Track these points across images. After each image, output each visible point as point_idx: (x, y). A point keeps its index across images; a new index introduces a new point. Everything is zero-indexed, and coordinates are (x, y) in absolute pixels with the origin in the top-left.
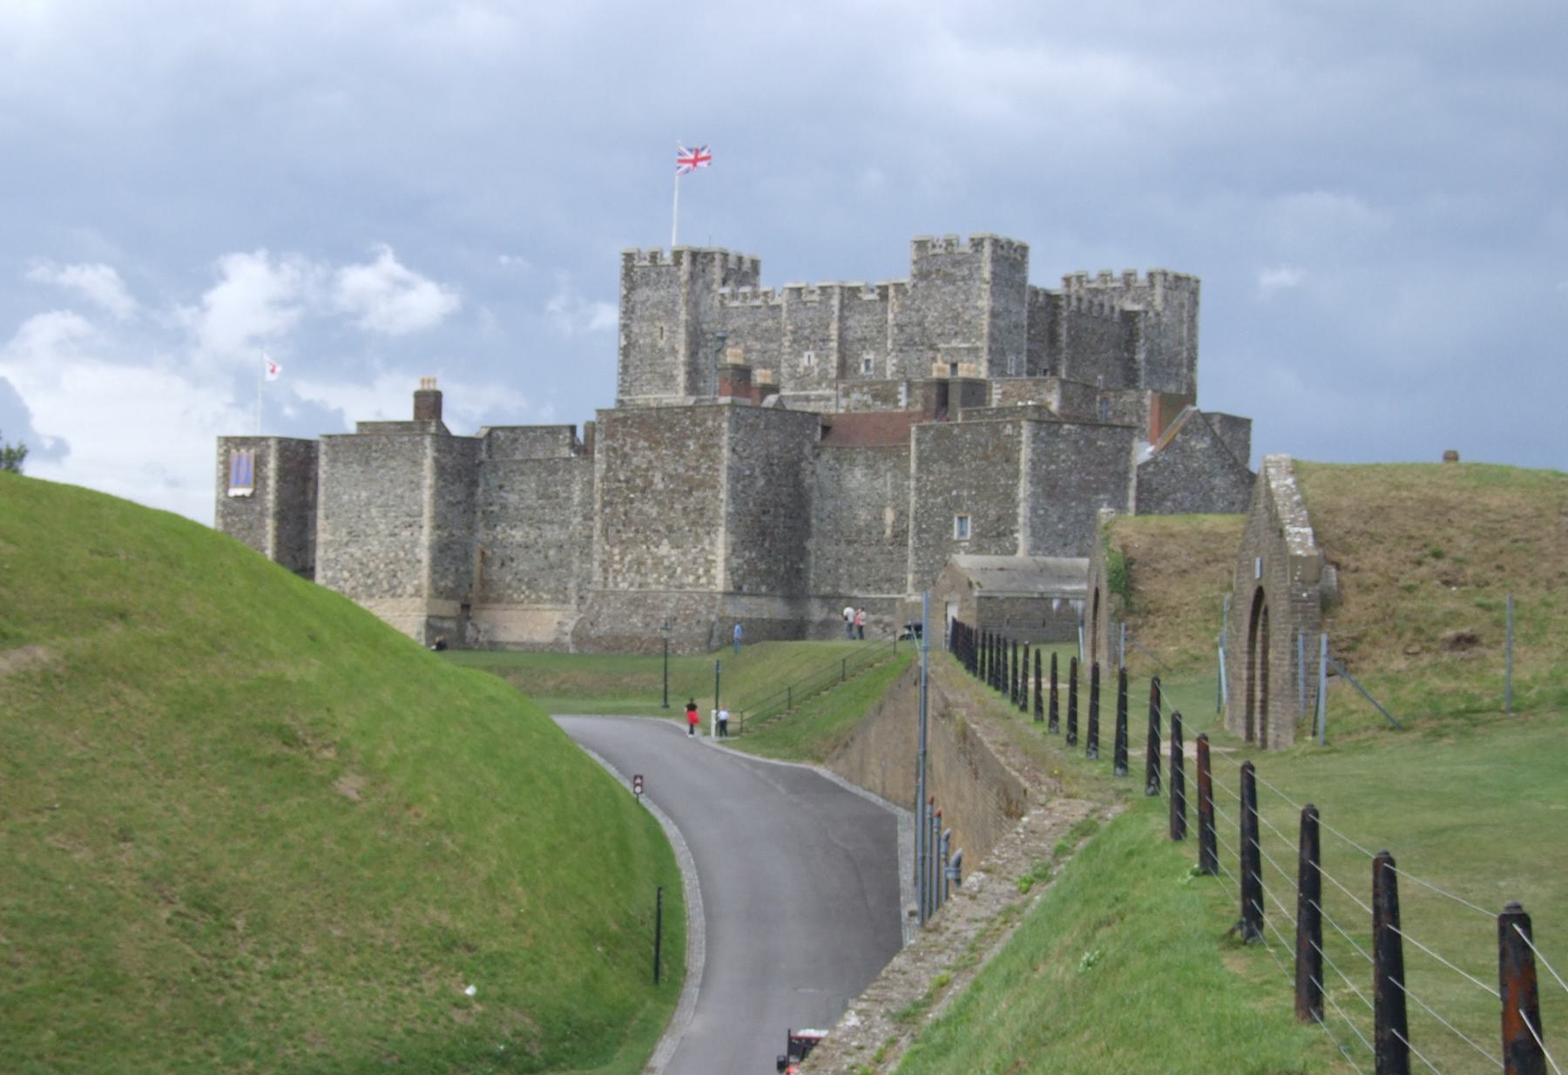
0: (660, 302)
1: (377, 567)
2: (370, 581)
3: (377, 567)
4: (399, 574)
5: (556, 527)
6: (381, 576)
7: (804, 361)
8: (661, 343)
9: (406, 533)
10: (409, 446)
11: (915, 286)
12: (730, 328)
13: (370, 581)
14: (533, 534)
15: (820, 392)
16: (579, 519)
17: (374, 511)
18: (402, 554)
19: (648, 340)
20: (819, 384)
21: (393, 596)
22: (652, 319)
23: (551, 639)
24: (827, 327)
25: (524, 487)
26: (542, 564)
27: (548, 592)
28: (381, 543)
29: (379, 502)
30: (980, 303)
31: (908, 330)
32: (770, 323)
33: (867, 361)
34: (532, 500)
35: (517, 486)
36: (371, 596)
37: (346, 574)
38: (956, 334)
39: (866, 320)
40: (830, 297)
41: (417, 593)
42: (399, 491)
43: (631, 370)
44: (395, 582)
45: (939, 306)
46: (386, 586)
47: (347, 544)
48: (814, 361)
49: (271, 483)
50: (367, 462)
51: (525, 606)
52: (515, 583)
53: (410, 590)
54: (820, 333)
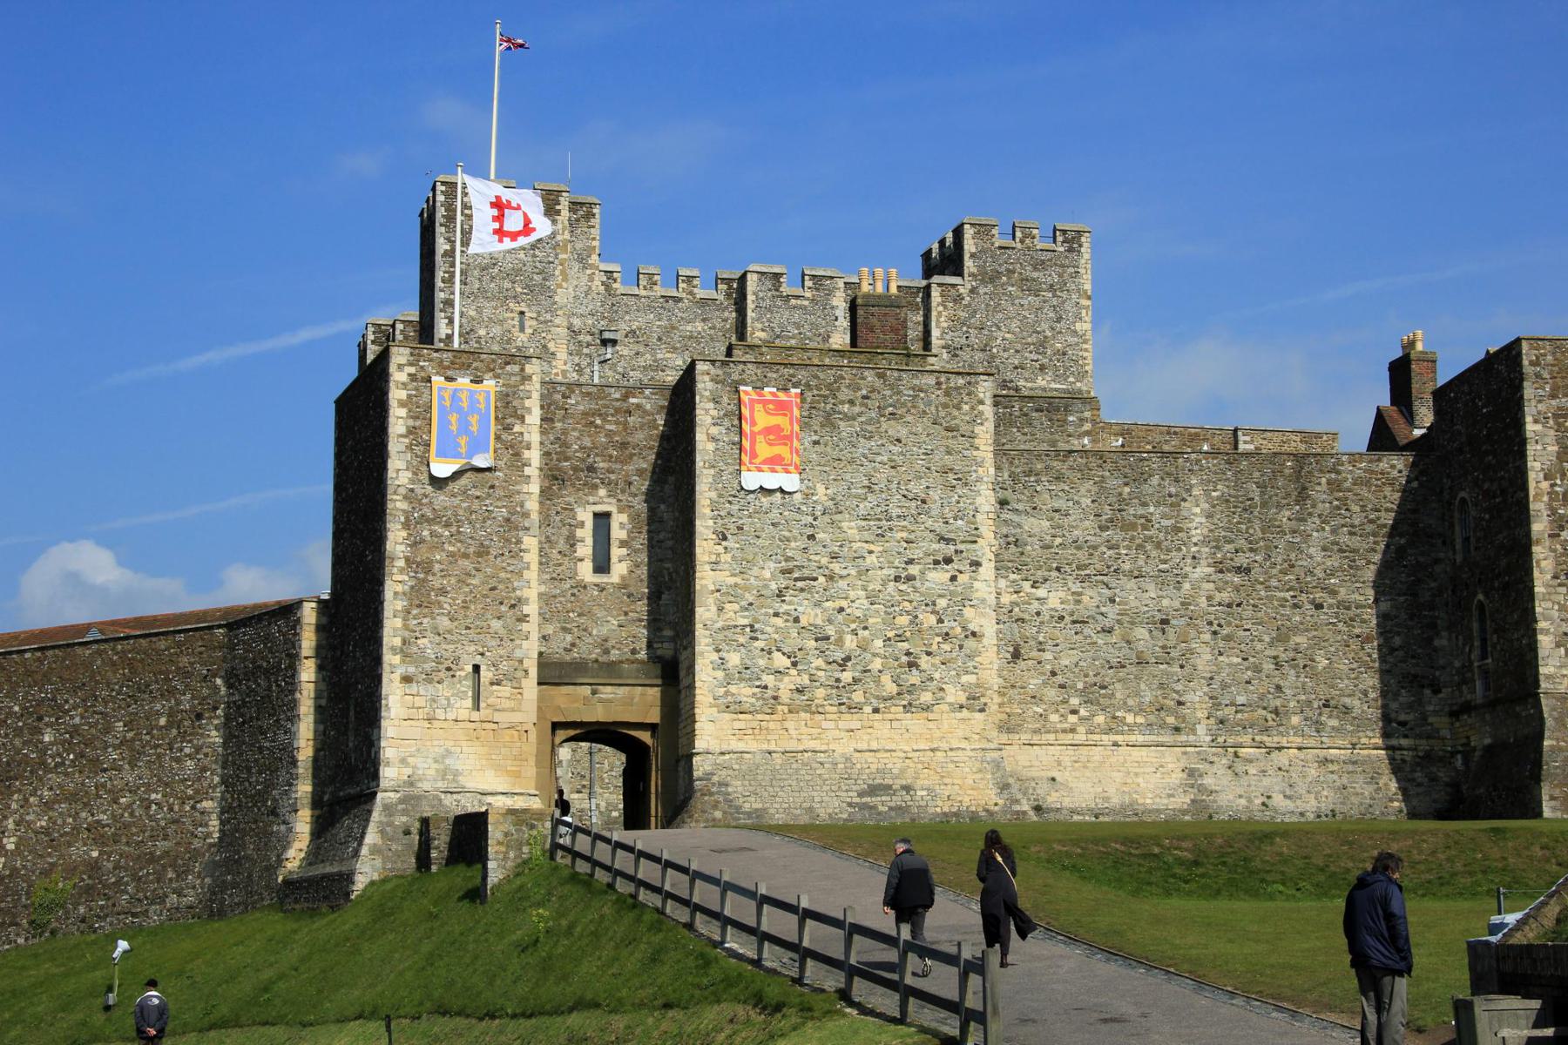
0: (518, 272)
1: (863, 647)
2: (847, 677)
3: (863, 647)
4: (924, 662)
5: (1151, 587)
6: (877, 664)
9: (939, 577)
10: (937, 396)
11: (973, 291)
13: (847, 677)
14: (1091, 598)
16: (1204, 570)
17: (850, 527)
18: (933, 619)
19: (496, 330)
21: (908, 708)
22: (504, 298)
23: (1182, 800)
25: (1060, 503)
26: (1114, 656)
27: (1140, 710)
28: (872, 599)
29: (864, 507)
30: (1078, 326)
31: (965, 355)
32: (699, 326)
34: (1085, 529)
35: (1046, 502)
36: (855, 708)
37: (781, 661)
38: (1042, 368)
40: (830, 293)
41: (974, 701)
42: (917, 488)
44: (914, 678)
45: (1014, 325)
46: (892, 688)
47: (780, 594)
49: (534, 456)
50: (829, 422)
51: (1080, 737)
52: (1051, 694)
53: (954, 695)
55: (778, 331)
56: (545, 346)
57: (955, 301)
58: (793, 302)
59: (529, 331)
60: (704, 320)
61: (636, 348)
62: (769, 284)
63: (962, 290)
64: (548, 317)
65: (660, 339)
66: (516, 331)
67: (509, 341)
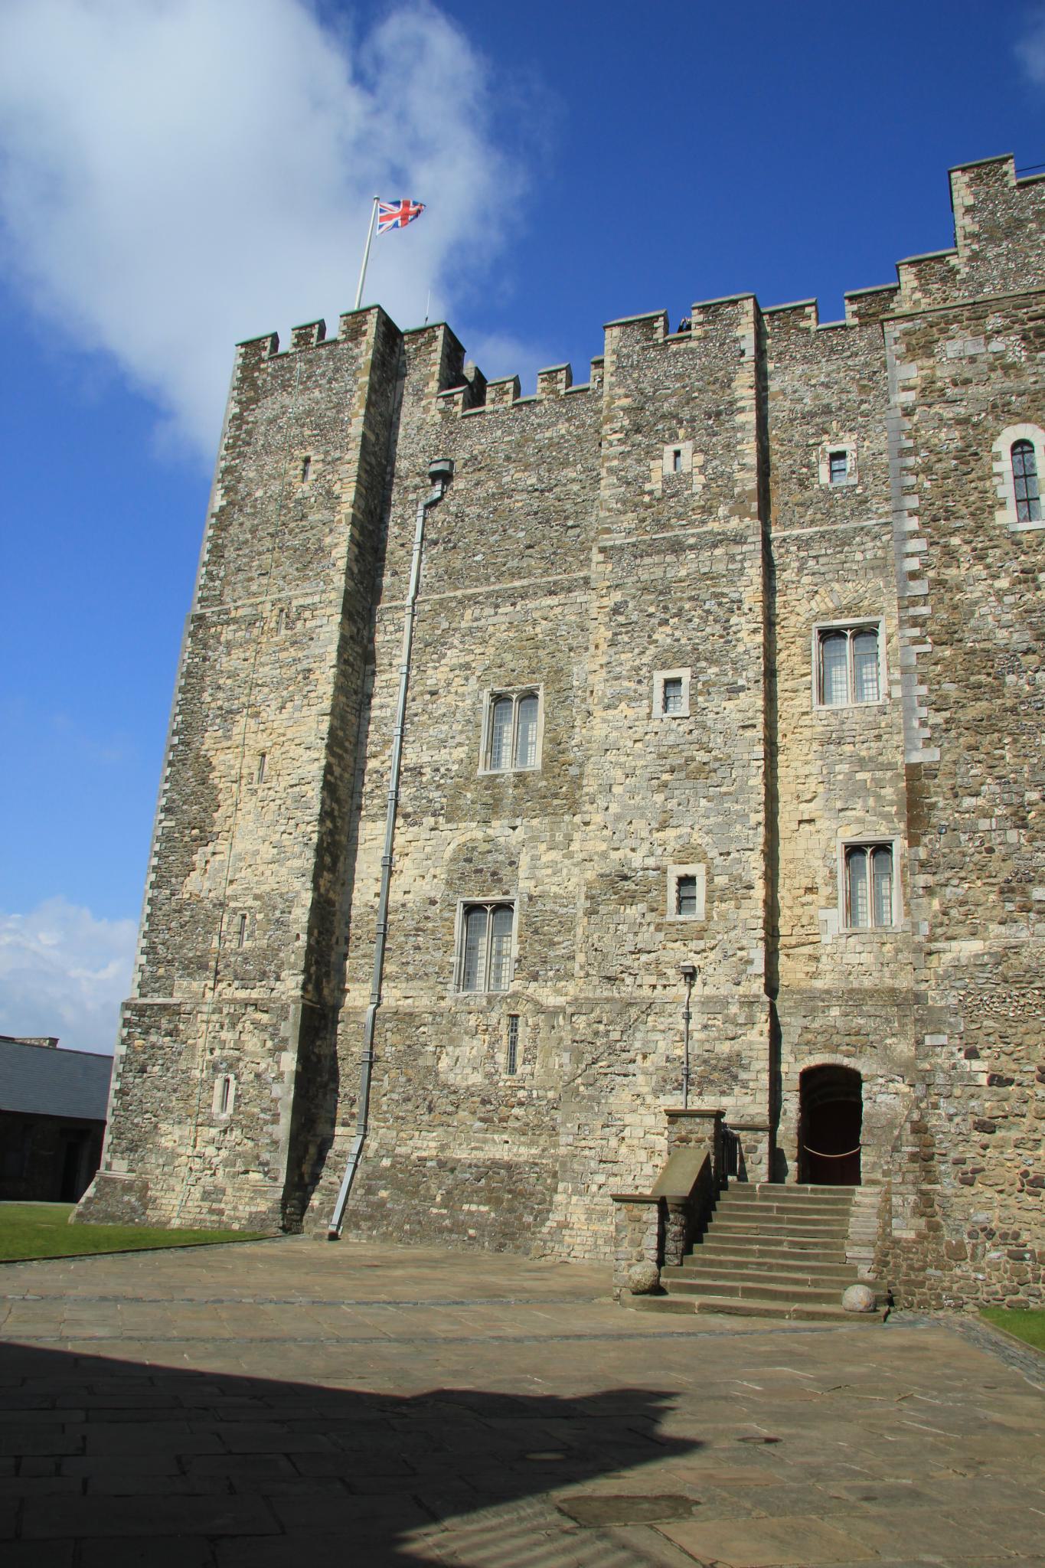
7: (664, 466)
8: (303, 489)
12: (461, 456)
15: (713, 526)
19: (275, 487)
20: (708, 510)
24: (728, 384)
32: (562, 428)
33: (840, 456)
39: (822, 370)
40: (734, 323)
43: (230, 553)
48: (687, 462)
54: (707, 401)
55: (649, 390)
56: (329, 492)
57: (943, 280)
58: (674, 347)
59: (311, 477)
60: (568, 420)
61: (476, 476)
62: (637, 335)
63: (953, 261)
64: (337, 454)
65: (508, 459)
66: (296, 482)
67: (288, 497)
